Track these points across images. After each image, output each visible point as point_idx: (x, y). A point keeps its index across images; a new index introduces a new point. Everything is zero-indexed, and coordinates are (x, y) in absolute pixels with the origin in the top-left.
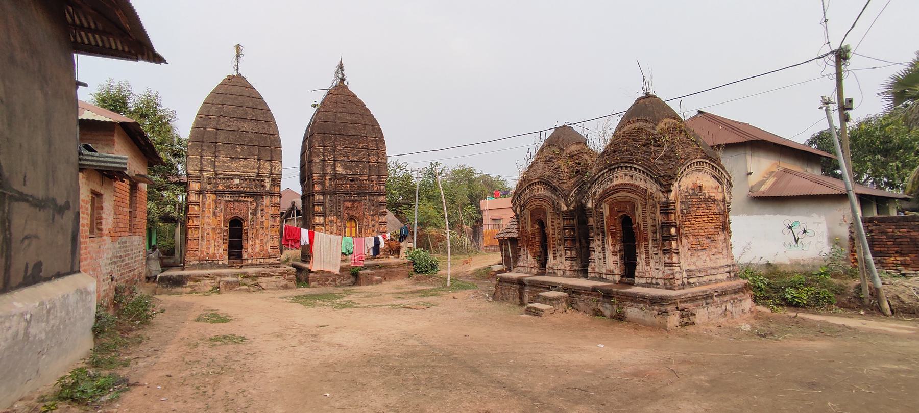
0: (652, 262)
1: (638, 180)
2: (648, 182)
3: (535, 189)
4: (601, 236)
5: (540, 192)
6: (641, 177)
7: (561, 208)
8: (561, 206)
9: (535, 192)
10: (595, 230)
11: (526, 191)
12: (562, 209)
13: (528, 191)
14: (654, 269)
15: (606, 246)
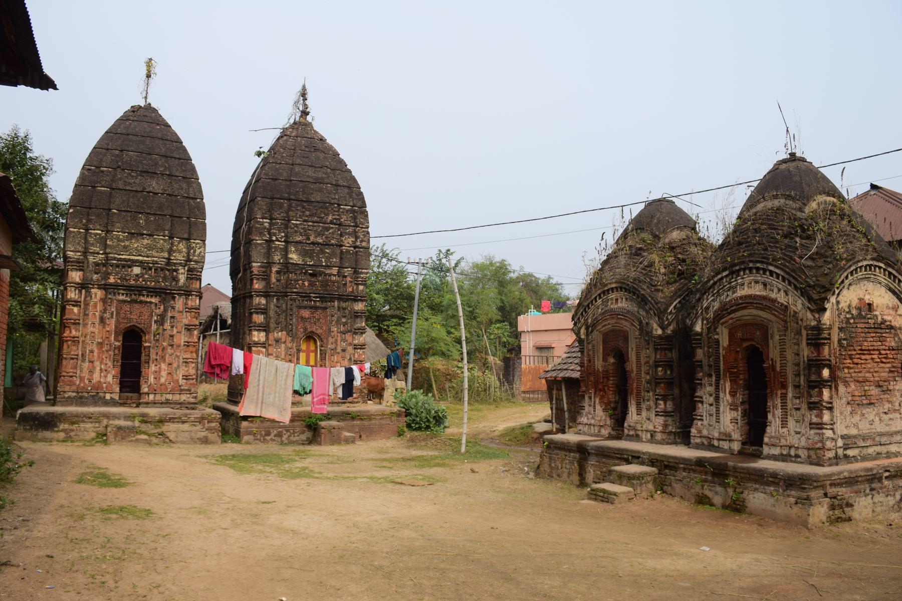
0: (791, 423)
1: (776, 290)
2: (790, 294)
3: (612, 299)
4: (714, 378)
5: (620, 305)
6: (780, 286)
7: (651, 332)
8: (652, 328)
9: (612, 303)
10: (706, 368)
11: (596, 301)
12: (654, 332)
13: (599, 301)
14: (793, 433)
15: (721, 395)
